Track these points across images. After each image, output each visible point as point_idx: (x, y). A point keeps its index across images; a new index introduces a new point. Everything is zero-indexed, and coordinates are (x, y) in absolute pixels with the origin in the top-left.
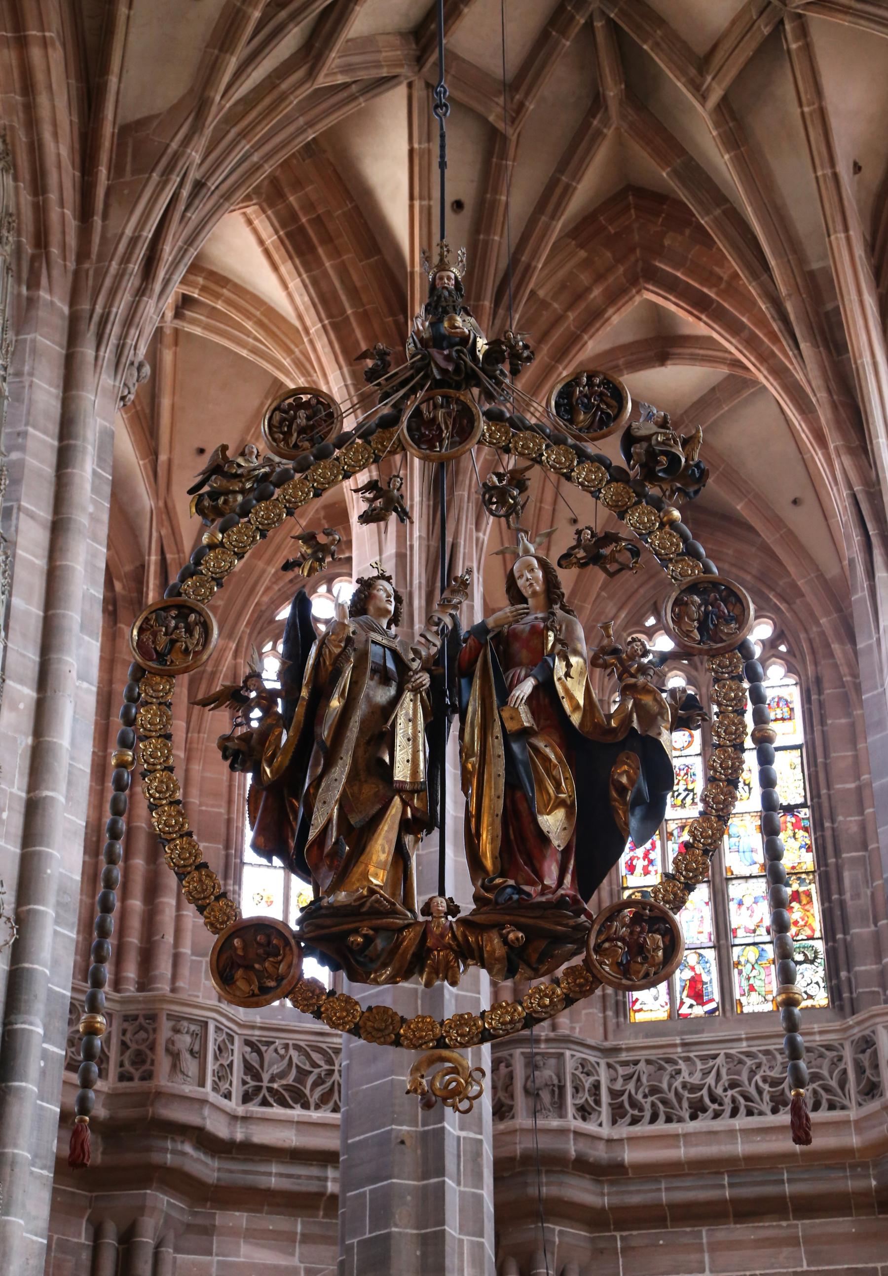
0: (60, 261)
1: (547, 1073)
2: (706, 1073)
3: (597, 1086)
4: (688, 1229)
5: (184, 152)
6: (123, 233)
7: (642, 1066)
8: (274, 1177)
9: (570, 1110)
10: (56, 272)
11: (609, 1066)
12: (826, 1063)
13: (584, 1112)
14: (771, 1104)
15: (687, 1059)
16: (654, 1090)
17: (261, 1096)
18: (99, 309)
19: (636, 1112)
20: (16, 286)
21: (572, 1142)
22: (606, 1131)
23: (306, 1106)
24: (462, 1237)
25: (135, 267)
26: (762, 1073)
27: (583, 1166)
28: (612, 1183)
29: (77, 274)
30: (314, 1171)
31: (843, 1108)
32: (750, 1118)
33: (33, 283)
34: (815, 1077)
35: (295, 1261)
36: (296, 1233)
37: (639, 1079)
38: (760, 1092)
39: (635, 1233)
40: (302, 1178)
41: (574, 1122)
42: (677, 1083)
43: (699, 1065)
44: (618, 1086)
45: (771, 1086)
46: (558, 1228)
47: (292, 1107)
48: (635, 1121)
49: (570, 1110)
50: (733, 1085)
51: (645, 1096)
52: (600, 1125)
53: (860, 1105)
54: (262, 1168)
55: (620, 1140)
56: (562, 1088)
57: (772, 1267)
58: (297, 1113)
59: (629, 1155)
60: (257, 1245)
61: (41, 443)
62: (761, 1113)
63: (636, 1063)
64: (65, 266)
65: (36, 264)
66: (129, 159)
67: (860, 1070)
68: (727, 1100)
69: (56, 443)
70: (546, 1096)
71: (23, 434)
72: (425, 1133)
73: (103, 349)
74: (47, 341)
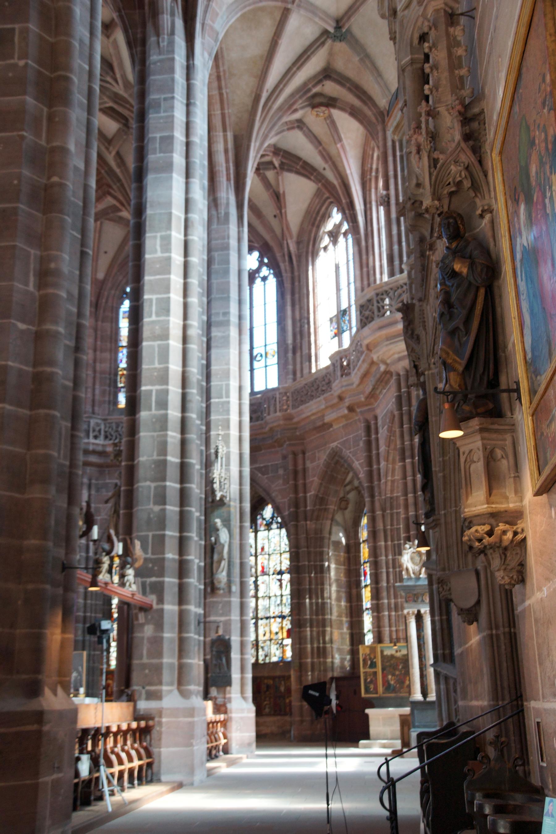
11: (105, 424)
13: (96, 437)
16: (117, 431)
27: (94, 452)
44: (107, 429)
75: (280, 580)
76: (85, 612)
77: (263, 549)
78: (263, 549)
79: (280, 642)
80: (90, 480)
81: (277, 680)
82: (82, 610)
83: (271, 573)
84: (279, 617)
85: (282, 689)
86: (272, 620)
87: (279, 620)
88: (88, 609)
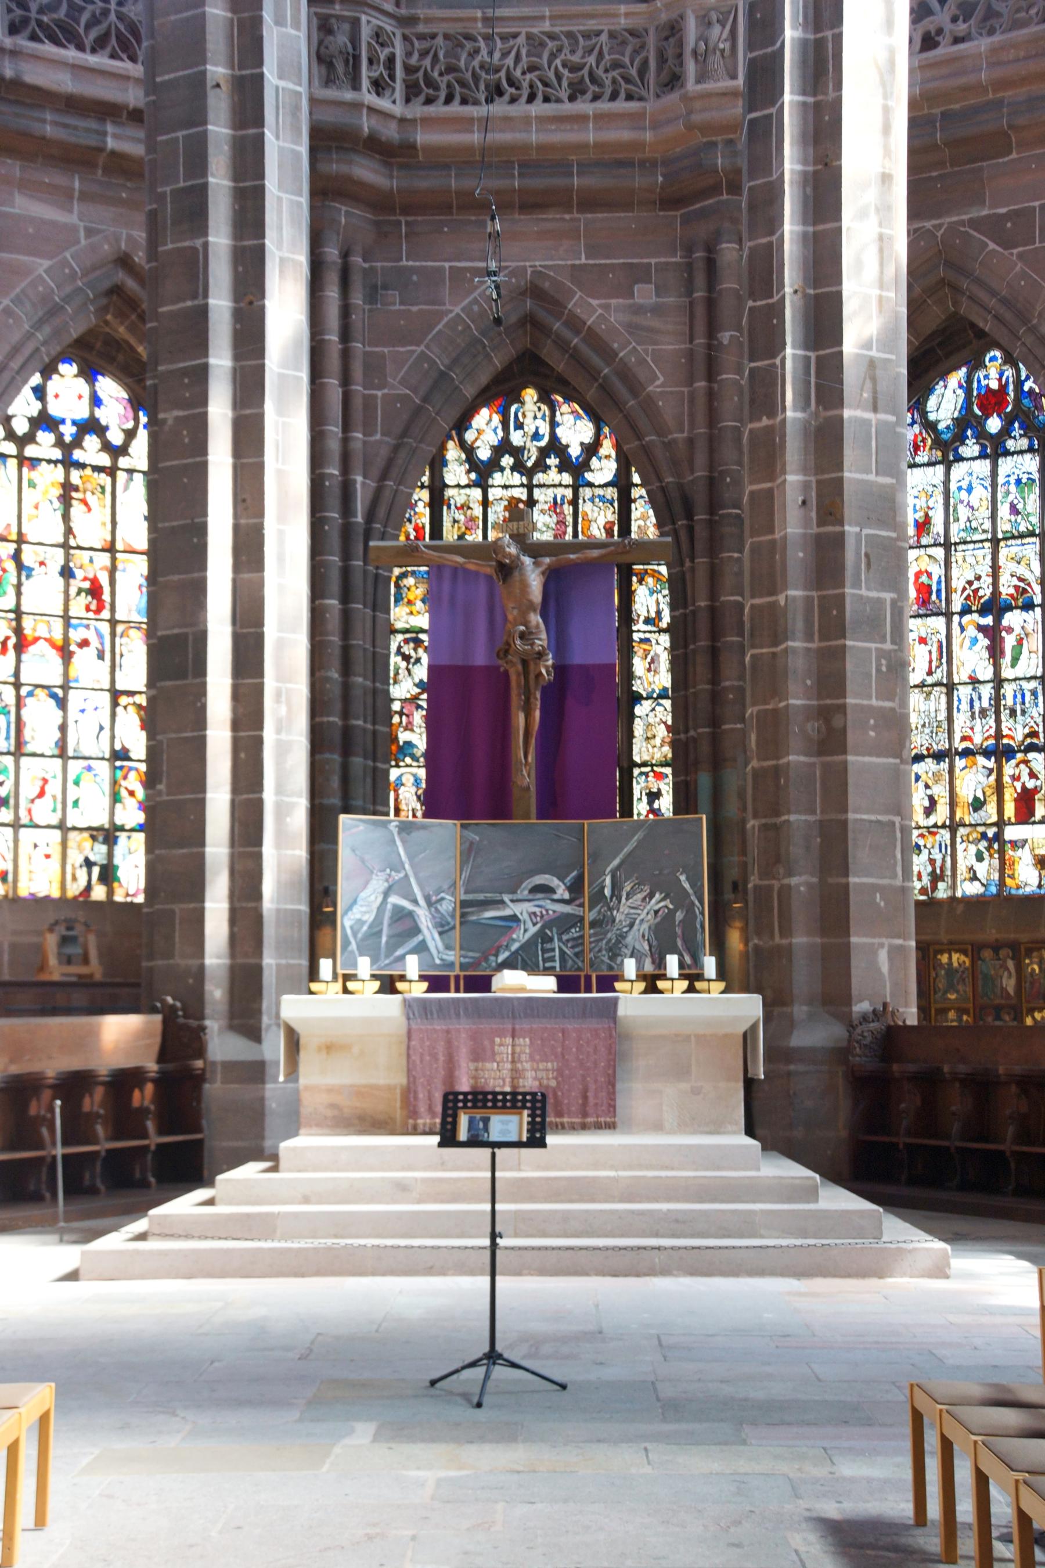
1: (341, 39)
2: (505, 55)
3: (391, 60)
4: (473, 218)
7: (440, 40)
8: (49, 126)
9: (365, 83)
11: (405, 38)
12: (629, 50)
13: (379, 86)
14: (569, 91)
15: (488, 38)
17: (30, 28)
19: (431, 91)
21: (365, 118)
22: (398, 110)
23: (81, 48)
24: (281, 194)
26: (563, 57)
28: (402, 166)
30: (93, 124)
31: (641, 99)
32: (547, 105)
34: (616, 65)
35: (72, 218)
36: (73, 189)
37: (436, 55)
38: (559, 77)
39: (420, 218)
40: (78, 131)
41: (369, 98)
42: (476, 63)
43: (499, 44)
44: (414, 61)
45: (571, 71)
46: (344, 208)
47: (64, 47)
48: (429, 101)
49: (365, 83)
50: (532, 68)
51: (441, 74)
52: (394, 102)
53: (658, 96)
54: (36, 114)
55: (413, 121)
56: (357, 58)
57: (552, 259)
58: (71, 54)
59: (421, 137)
60: (32, 197)
62: (559, 100)
63: (433, 36)
67: (662, 59)
68: (525, 85)
70: (340, 68)
72: (242, 77)
75: (994, 635)
76: (346, 715)
77: (923, 526)
78: (923, 526)
79: (990, 834)
80: (345, 255)
81: (987, 954)
82: (338, 706)
83: (956, 607)
84: (987, 753)
85: (1010, 984)
86: (960, 763)
87: (991, 764)
88: (357, 706)
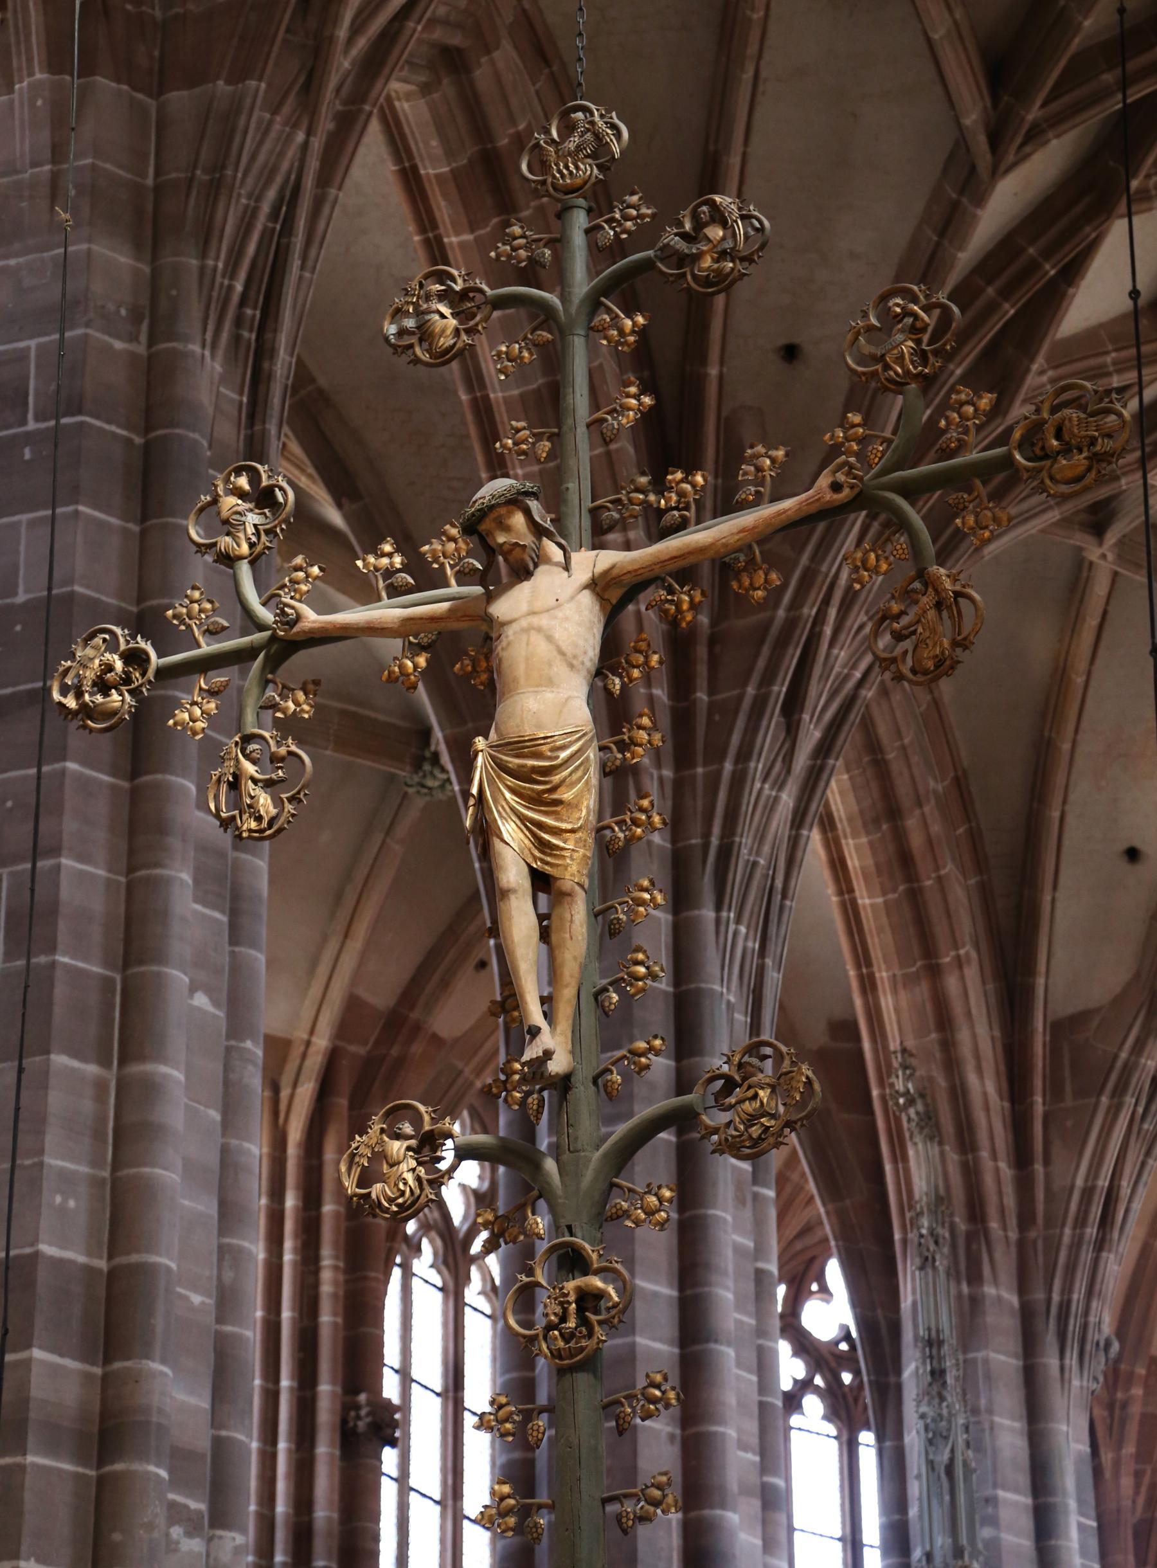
0: (1001, 1233)
5: (1136, 1063)
6: (1072, 1186)
10: (998, 1255)
18: (1056, 1297)
20: (952, 1284)
25: (1091, 1231)
29: (1021, 1244)
33: (975, 1277)
61: (1014, 1502)
64: (1007, 1237)
65: (974, 1247)
66: (1067, 1073)
69: (1029, 1501)
71: (992, 1501)
73: (1068, 1354)
74: (1001, 1357)
